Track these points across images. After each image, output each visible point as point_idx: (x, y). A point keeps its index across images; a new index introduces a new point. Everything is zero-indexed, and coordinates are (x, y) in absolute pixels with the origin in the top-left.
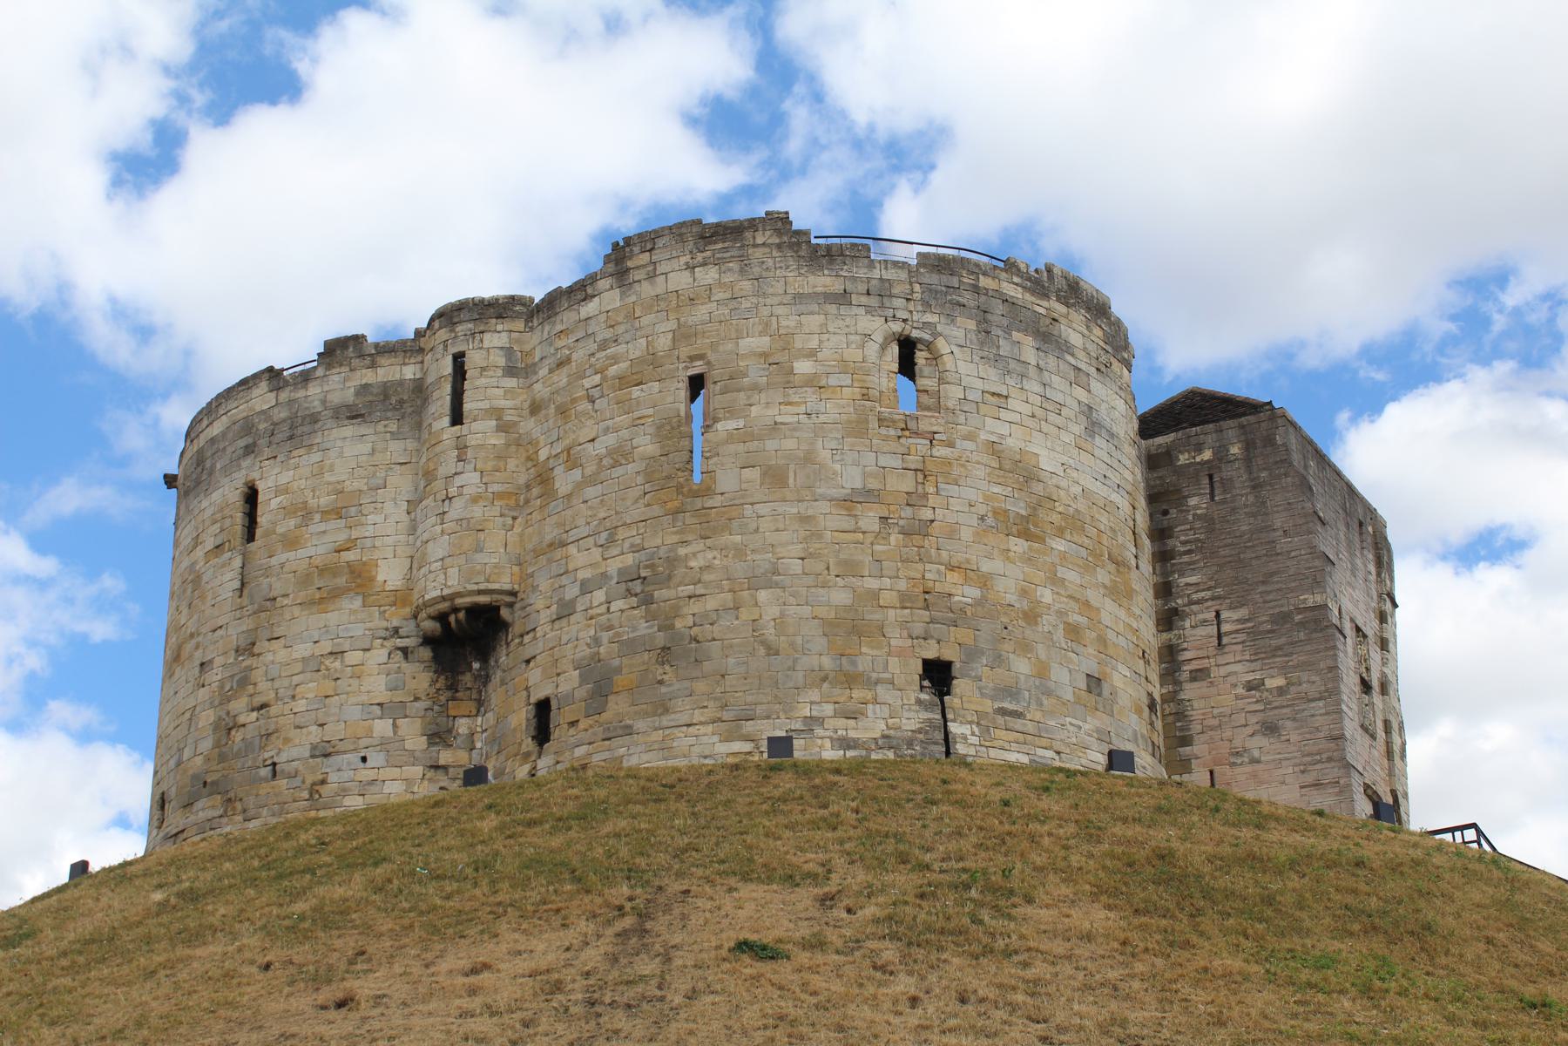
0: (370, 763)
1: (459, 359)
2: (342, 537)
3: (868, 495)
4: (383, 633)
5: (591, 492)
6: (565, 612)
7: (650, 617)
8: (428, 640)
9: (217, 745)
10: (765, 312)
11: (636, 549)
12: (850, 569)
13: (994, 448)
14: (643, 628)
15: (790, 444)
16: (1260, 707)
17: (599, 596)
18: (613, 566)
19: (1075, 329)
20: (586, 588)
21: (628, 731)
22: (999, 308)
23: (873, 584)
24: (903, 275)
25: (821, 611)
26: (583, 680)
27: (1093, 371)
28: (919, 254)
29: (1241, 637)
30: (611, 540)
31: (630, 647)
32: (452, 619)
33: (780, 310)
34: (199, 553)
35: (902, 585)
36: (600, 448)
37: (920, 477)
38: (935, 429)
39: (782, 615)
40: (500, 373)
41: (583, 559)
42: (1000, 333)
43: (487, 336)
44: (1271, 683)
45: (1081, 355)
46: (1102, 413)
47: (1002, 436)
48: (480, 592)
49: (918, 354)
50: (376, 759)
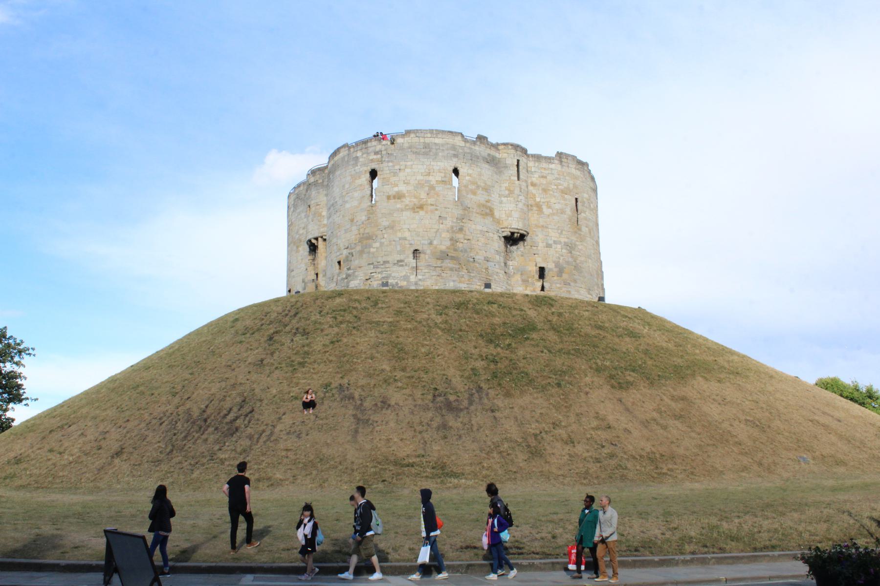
1: (518, 161)
2: (487, 198)
5: (556, 217)
6: (549, 246)
7: (572, 257)
8: (505, 238)
9: (453, 245)
11: (568, 238)
14: (570, 259)
17: (559, 246)
18: (563, 240)
20: (555, 242)
21: (569, 284)
26: (556, 267)
30: (561, 233)
31: (568, 263)
32: (516, 235)
34: (431, 178)
36: (557, 206)
41: (554, 235)
50: (497, 266)
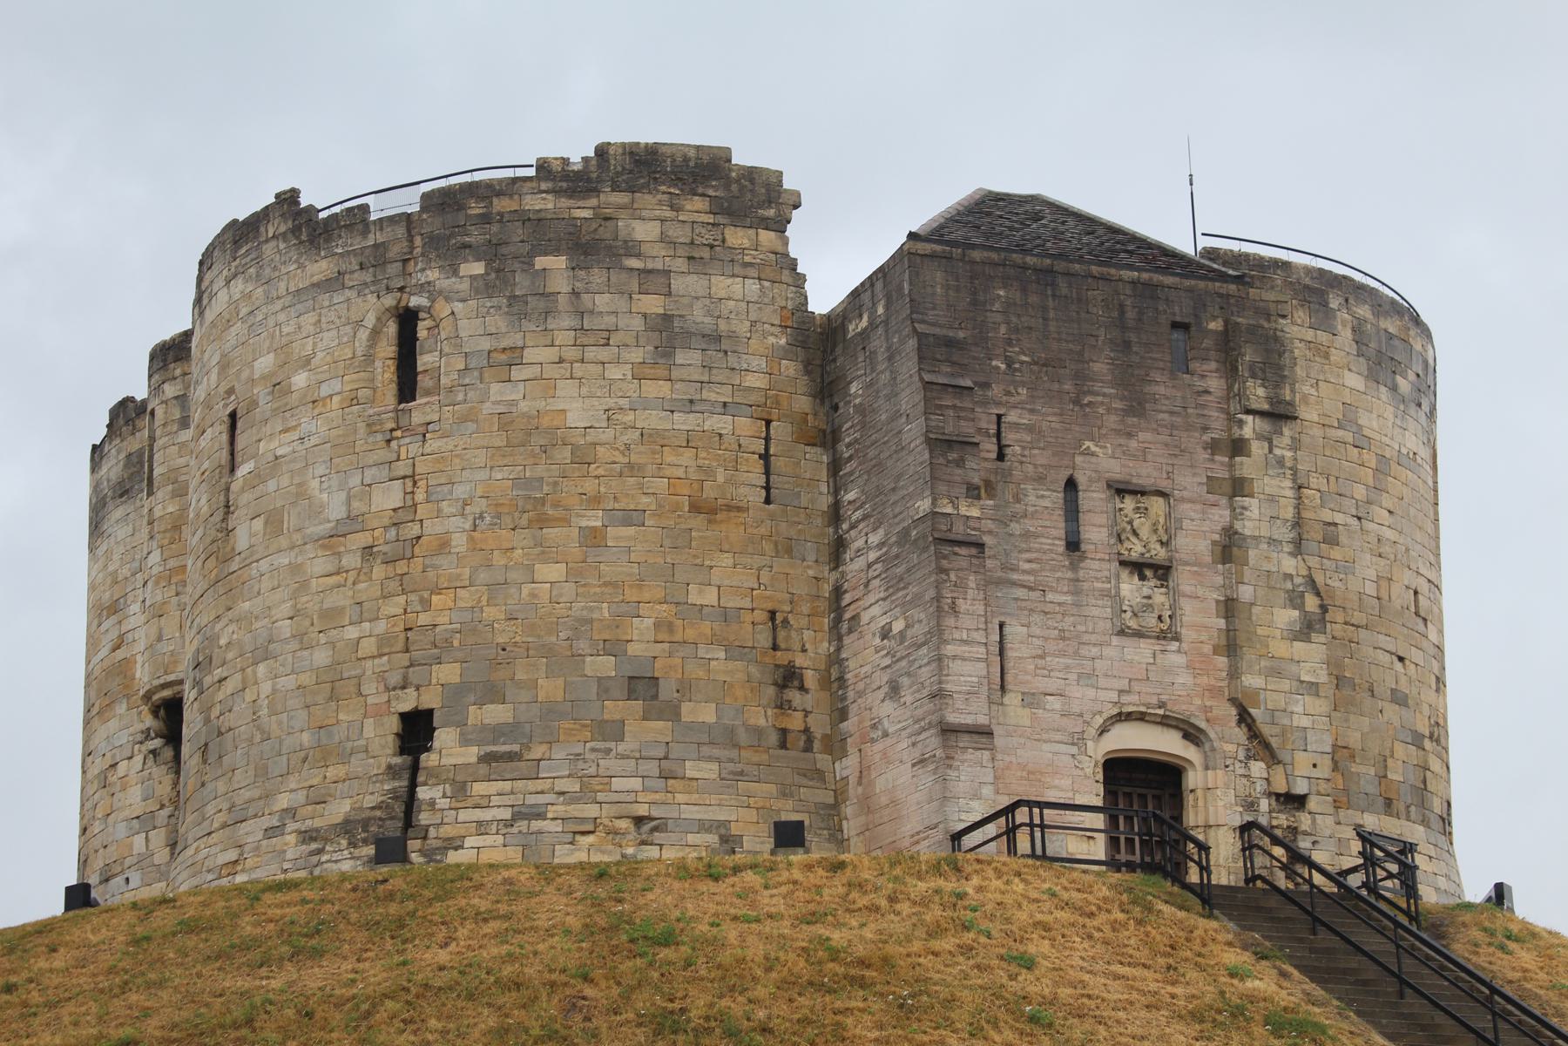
0: (132, 885)
3: (353, 522)
4: (139, 737)
10: (271, 322)
12: (331, 616)
13: (505, 420)
15: (285, 481)
16: (887, 661)
19: (645, 224)
22: (518, 232)
23: (352, 633)
24: (401, 231)
25: (306, 679)
27: (680, 264)
28: (426, 197)
29: (879, 566)
33: (282, 317)
35: (381, 627)
37: (409, 483)
38: (428, 419)
39: (274, 691)
40: (175, 428)
42: (517, 265)
43: (166, 386)
44: (898, 626)
45: (659, 250)
46: (698, 316)
47: (514, 403)
48: (164, 686)
49: (421, 325)
